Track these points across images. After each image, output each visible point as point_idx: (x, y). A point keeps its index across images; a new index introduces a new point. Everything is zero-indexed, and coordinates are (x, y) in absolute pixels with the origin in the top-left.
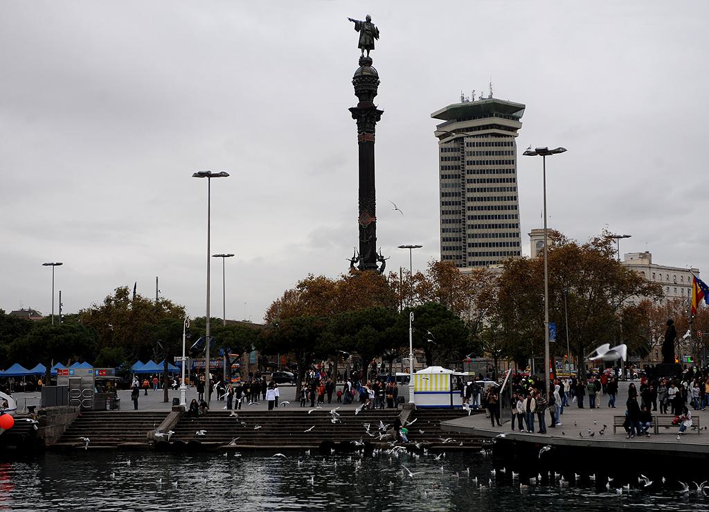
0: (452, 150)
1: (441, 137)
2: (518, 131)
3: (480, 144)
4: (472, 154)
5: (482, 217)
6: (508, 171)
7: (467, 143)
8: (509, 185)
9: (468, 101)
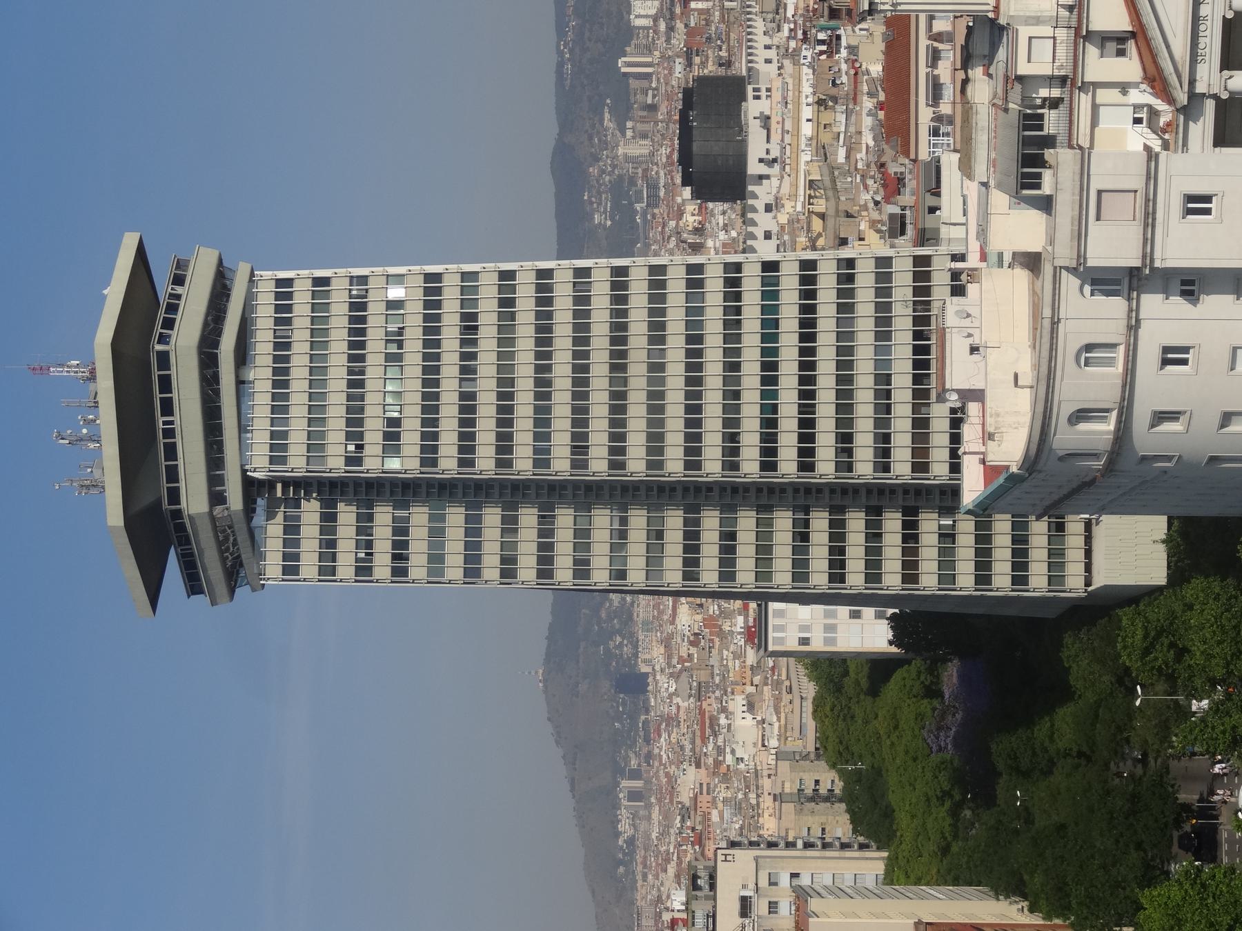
3: (280, 407)
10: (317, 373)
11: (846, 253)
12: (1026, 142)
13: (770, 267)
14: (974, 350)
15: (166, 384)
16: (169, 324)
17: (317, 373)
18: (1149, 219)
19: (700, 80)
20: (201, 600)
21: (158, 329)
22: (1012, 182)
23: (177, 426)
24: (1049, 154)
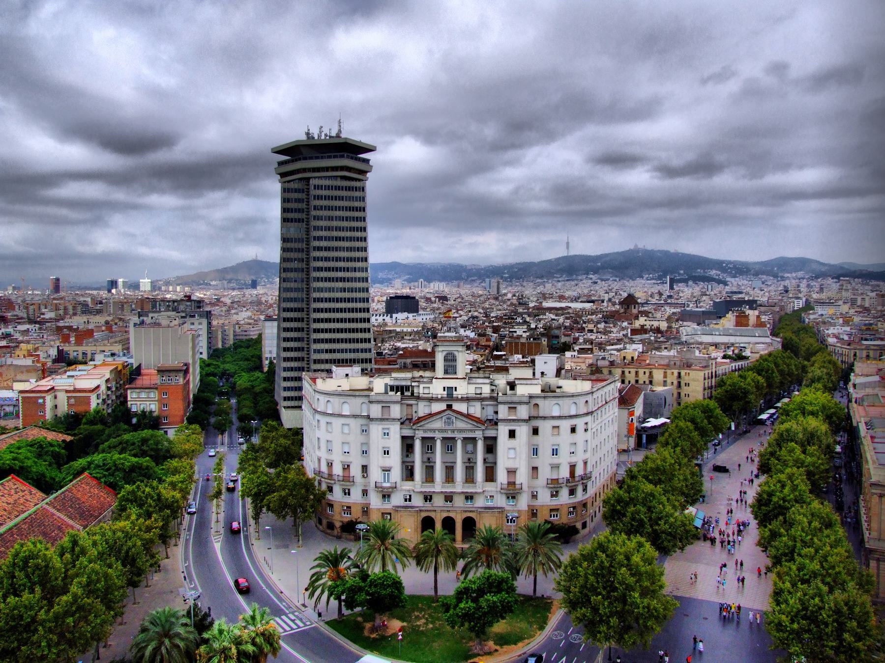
0: (296, 191)
1: (283, 175)
2: (368, 175)
3: (328, 188)
4: (319, 198)
5: (327, 310)
6: (358, 219)
7: (315, 186)
8: (360, 264)
9: (313, 138)
11: (372, 340)
12: (402, 387)
13: (369, 320)
14: (347, 375)
16: (352, 158)
18: (382, 420)
19: (418, 301)
20: (276, 166)
24: (399, 393)
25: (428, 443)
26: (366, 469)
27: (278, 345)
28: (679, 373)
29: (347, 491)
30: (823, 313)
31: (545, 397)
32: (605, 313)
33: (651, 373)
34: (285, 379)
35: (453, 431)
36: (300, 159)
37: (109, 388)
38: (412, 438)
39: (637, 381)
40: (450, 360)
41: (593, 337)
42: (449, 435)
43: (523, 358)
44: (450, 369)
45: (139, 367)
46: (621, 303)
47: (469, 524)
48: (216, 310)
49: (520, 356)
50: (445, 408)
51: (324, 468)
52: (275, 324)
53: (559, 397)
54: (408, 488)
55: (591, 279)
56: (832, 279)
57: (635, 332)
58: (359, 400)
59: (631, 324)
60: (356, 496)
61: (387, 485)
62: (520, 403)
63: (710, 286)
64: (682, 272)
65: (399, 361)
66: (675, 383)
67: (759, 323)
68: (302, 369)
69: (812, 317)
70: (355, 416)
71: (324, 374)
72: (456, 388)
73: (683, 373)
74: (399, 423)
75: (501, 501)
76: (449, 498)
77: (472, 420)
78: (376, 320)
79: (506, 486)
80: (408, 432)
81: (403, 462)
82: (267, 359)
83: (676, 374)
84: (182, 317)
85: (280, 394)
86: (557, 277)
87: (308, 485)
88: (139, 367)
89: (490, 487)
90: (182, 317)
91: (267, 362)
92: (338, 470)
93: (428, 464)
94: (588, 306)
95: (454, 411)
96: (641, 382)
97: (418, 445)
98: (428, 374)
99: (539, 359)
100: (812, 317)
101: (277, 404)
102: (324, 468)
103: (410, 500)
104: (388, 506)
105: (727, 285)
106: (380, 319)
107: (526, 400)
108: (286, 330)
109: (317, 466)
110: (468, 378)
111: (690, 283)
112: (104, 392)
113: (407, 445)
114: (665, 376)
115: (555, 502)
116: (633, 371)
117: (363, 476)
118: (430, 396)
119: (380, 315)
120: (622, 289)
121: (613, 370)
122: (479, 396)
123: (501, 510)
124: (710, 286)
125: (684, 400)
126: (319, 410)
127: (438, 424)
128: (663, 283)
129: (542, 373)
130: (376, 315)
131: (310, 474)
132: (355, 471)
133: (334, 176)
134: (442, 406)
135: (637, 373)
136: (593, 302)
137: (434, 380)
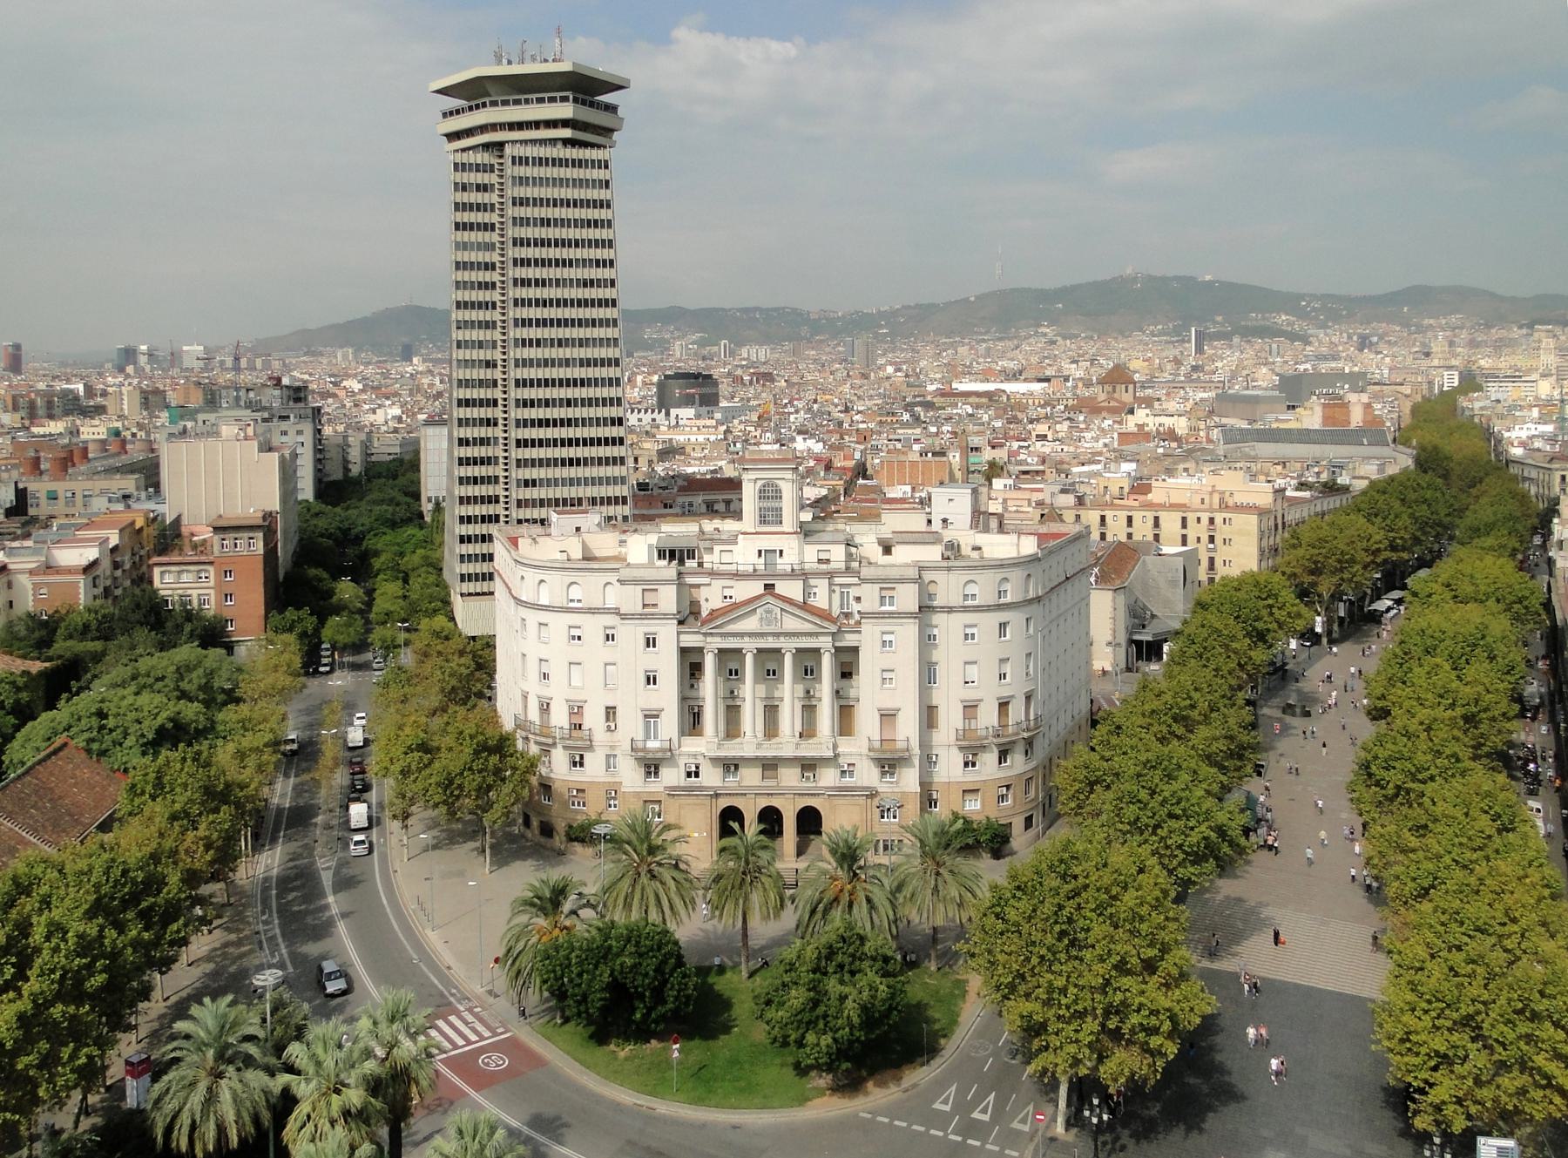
2: (616, 135)
3: (541, 162)
7: (514, 158)
10: (561, 182)
12: (681, 551)
14: (578, 529)
15: (553, 100)
16: (584, 103)
17: (561, 182)
18: (642, 617)
19: (716, 384)
21: (580, 96)
22: (661, 545)
23: (531, 106)
24: (675, 562)
25: (730, 660)
26: (614, 713)
27: (450, 473)
28: (1212, 521)
29: (578, 759)
30: (1500, 396)
31: (949, 569)
32: (1070, 403)
33: (1157, 519)
34: (462, 540)
35: (777, 635)
36: (484, 105)
37: (116, 566)
38: (700, 650)
39: (1130, 536)
40: (769, 493)
41: (1047, 450)
42: (770, 643)
43: (913, 489)
44: (769, 517)
45: (177, 521)
46: (1101, 382)
47: (810, 821)
48: (329, 406)
49: (908, 488)
50: (762, 591)
51: (534, 715)
52: (445, 430)
53: (975, 568)
54: (693, 750)
55: (1045, 335)
56: (1520, 327)
57: (1123, 437)
58: (599, 579)
59: (1120, 423)
60: (594, 763)
61: (652, 744)
62: (902, 581)
63: (1274, 346)
64: (1219, 319)
65: (680, 500)
66: (1205, 538)
67: (1369, 418)
68: (497, 519)
69: (1477, 405)
70: (592, 611)
71: (537, 529)
72: (781, 552)
73: (1219, 518)
74: (675, 622)
75: (867, 775)
76: (770, 765)
77: (813, 614)
78: (640, 420)
79: (877, 745)
80: (691, 640)
81: (683, 699)
82: (429, 500)
83: (1205, 521)
84: (265, 420)
85: (453, 568)
86: (981, 334)
87: (501, 746)
88: (177, 521)
89: (846, 746)
90: (265, 420)
91: (430, 506)
92: (560, 718)
93: (731, 703)
94: (1037, 387)
95: (779, 597)
96: (1137, 537)
97: (709, 663)
98: (729, 525)
99: (940, 496)
100: (1477, 405)
101: (443, 586)
102: (534, 715)
103: (697, 775)
104: (656, 786)
105: (1310, 343)
106: (647, 418)
107: (913, 573)
108: (463, 442)
109: (519, 710)
110: (805, 532)
111: (1236, 340)
112: (108, 573)
113: (691, 665)
114: (1184, 526)
115: (971, 777)
116: (1123, 515)
117: (609, 727)
118: (734, 567)
119: (646, 411)
120: (1104, 355)
121: (1082, 513)
122: (824, 566)
123: (872, 794)
124: (1274, 346)
125: (1221, 571)
126: (524, 599)
127: (750, 624)
128: (1183, 341)
129: (945, 521)
130: (639, 411)
131: (508, 725)
132: (593, 719)
133: (550, 140)
134: (757, 588)
135: (1130, 519)
136: (1047, 380)
137: (740, 537)
